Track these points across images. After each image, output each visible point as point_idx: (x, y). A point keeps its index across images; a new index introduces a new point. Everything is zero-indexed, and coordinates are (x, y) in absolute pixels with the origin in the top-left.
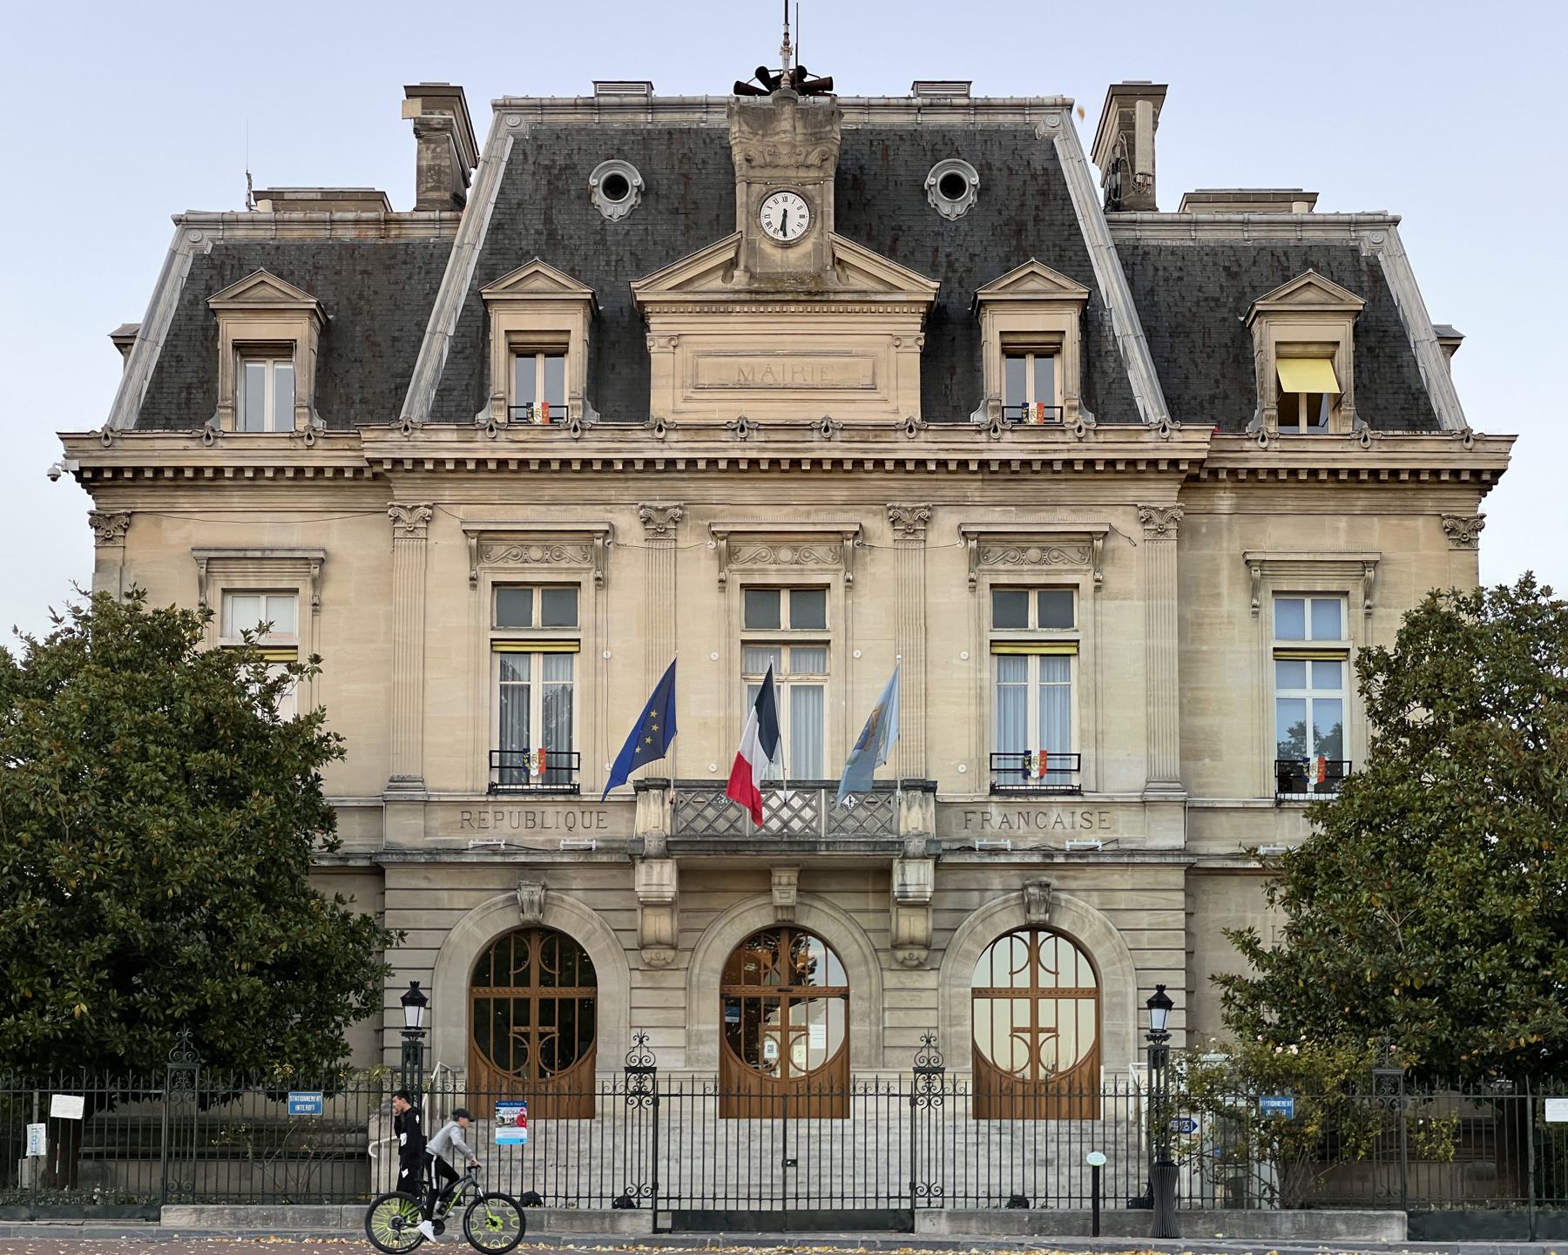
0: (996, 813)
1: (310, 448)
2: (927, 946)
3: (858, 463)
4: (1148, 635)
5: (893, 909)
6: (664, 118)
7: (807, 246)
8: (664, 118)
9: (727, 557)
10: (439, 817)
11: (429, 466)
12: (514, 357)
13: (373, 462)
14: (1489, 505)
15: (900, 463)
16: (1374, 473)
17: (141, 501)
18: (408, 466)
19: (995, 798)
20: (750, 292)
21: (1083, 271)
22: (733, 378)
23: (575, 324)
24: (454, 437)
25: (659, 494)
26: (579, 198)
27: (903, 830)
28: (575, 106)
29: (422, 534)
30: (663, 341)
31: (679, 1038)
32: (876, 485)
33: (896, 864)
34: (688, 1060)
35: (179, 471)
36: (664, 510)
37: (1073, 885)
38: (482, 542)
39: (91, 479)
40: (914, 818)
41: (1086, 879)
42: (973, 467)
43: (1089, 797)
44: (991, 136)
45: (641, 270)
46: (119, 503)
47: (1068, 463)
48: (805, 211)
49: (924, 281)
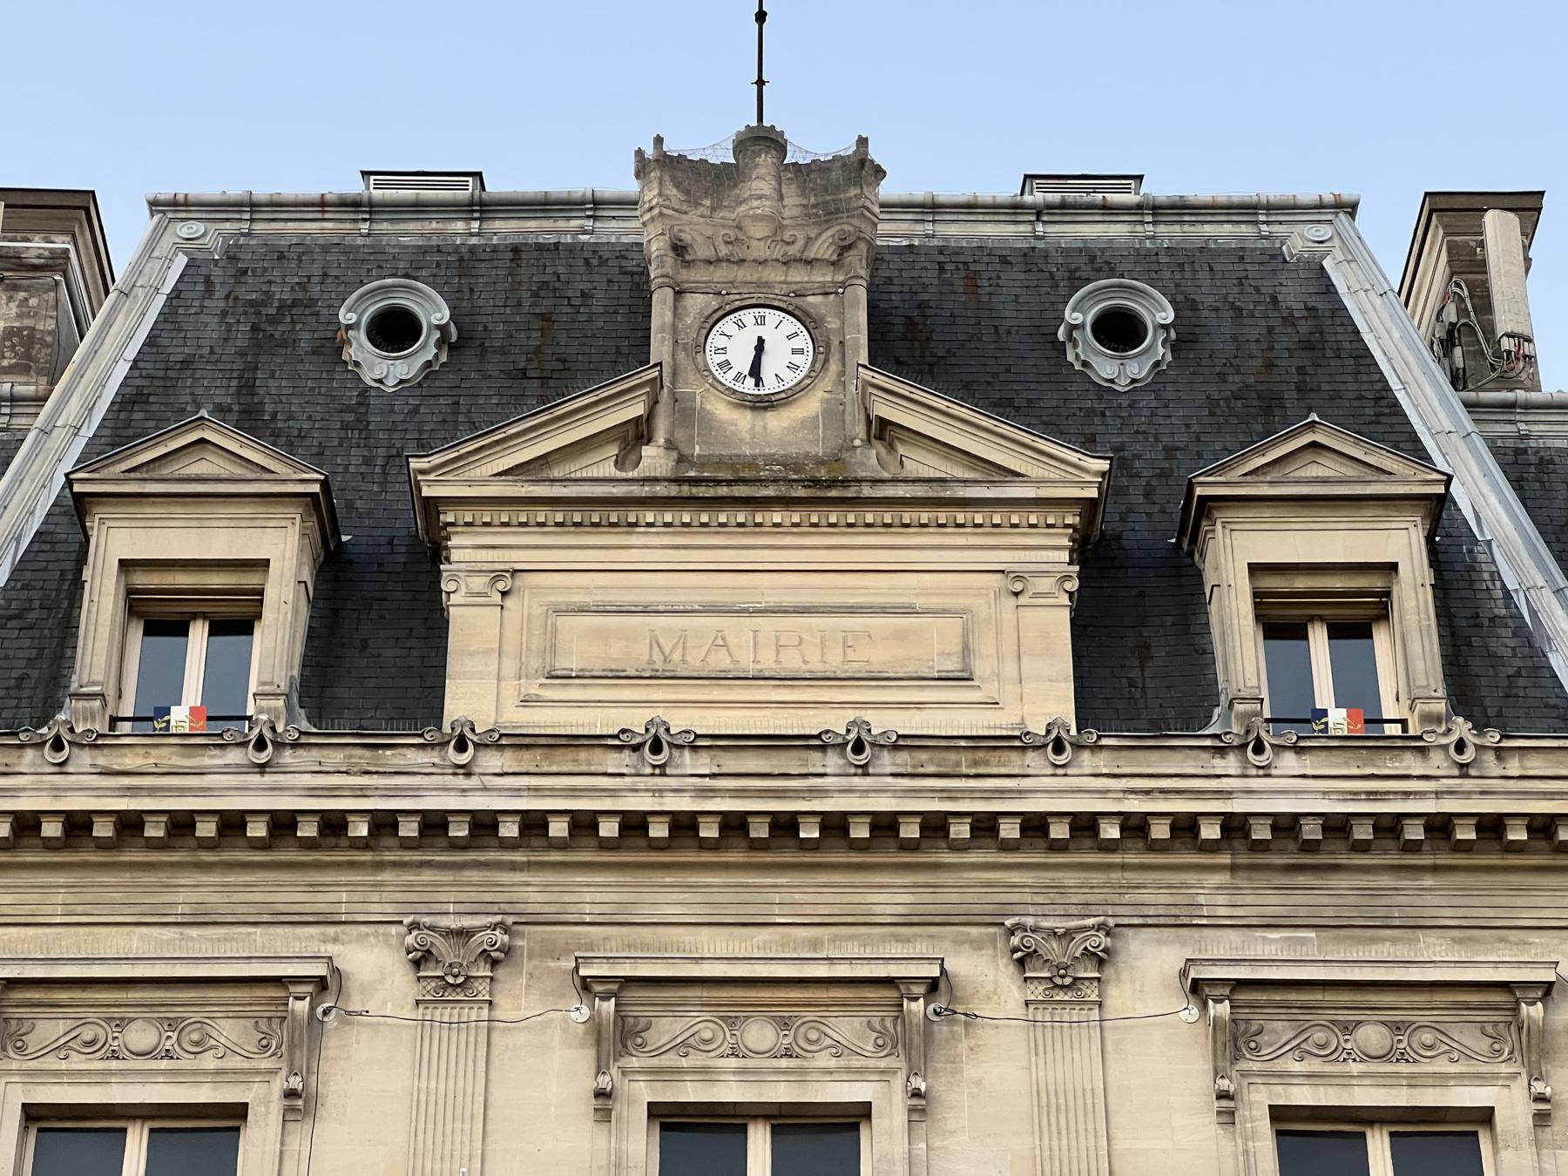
3: (935, 826)
6: (504, 228)
8: (504, 228)
15: (1035, 825)
20: (678, 481)
22: (637, 656)
23: (282, 551)
26: (315, 352)
30: (479, 583)
32: (975, 881)
36: (464, 934)
42: (1211, 831)
47: (1440, 826)
48: (804, 341)
49: (1073, 457)
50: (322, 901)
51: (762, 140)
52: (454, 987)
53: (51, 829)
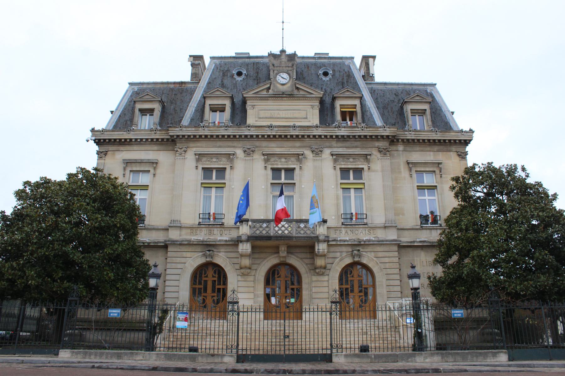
0: (343, 230)
1: (155, 133)
2: (325, 268)
3: (303, 136)
4: (383, 182)
5: (315, 257)
6: (252, 60)
7: (289, 85)
9: (266, 161)
10: (184, 231)
11: (186, 137)
12: (212, 113)
13: (172, 136)
14: (468, 148)
15: (314, 136)
16: (439, 140)
17: (111, 148)
18: (181, 137)
19: (343, 226)
21: (360, 91)
22: (269, 116)
23: (227, 103)
24: (193, 129)
25: (248, 144)
27: (318, 233)
28: (231, 57)
29: (183, 155)
31: (252, 296)
32: (307, 142)
33: (316, 244)
34: (254, 302)
35: (120, 140)
37: (366, 250)
38: (200, 157)
39: (98, 142)
40: (322, 231)
41: (370, 248)
42: (334, 137)
43: (370, 225)
44: (334, 64)
45: (244, 90)
46: (104, 149)
47: (360, 136)
50: (234, 145)
51: (283, 51)
52: (249, 155)
53: (203, 137)
